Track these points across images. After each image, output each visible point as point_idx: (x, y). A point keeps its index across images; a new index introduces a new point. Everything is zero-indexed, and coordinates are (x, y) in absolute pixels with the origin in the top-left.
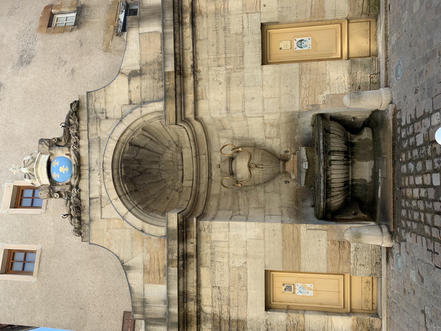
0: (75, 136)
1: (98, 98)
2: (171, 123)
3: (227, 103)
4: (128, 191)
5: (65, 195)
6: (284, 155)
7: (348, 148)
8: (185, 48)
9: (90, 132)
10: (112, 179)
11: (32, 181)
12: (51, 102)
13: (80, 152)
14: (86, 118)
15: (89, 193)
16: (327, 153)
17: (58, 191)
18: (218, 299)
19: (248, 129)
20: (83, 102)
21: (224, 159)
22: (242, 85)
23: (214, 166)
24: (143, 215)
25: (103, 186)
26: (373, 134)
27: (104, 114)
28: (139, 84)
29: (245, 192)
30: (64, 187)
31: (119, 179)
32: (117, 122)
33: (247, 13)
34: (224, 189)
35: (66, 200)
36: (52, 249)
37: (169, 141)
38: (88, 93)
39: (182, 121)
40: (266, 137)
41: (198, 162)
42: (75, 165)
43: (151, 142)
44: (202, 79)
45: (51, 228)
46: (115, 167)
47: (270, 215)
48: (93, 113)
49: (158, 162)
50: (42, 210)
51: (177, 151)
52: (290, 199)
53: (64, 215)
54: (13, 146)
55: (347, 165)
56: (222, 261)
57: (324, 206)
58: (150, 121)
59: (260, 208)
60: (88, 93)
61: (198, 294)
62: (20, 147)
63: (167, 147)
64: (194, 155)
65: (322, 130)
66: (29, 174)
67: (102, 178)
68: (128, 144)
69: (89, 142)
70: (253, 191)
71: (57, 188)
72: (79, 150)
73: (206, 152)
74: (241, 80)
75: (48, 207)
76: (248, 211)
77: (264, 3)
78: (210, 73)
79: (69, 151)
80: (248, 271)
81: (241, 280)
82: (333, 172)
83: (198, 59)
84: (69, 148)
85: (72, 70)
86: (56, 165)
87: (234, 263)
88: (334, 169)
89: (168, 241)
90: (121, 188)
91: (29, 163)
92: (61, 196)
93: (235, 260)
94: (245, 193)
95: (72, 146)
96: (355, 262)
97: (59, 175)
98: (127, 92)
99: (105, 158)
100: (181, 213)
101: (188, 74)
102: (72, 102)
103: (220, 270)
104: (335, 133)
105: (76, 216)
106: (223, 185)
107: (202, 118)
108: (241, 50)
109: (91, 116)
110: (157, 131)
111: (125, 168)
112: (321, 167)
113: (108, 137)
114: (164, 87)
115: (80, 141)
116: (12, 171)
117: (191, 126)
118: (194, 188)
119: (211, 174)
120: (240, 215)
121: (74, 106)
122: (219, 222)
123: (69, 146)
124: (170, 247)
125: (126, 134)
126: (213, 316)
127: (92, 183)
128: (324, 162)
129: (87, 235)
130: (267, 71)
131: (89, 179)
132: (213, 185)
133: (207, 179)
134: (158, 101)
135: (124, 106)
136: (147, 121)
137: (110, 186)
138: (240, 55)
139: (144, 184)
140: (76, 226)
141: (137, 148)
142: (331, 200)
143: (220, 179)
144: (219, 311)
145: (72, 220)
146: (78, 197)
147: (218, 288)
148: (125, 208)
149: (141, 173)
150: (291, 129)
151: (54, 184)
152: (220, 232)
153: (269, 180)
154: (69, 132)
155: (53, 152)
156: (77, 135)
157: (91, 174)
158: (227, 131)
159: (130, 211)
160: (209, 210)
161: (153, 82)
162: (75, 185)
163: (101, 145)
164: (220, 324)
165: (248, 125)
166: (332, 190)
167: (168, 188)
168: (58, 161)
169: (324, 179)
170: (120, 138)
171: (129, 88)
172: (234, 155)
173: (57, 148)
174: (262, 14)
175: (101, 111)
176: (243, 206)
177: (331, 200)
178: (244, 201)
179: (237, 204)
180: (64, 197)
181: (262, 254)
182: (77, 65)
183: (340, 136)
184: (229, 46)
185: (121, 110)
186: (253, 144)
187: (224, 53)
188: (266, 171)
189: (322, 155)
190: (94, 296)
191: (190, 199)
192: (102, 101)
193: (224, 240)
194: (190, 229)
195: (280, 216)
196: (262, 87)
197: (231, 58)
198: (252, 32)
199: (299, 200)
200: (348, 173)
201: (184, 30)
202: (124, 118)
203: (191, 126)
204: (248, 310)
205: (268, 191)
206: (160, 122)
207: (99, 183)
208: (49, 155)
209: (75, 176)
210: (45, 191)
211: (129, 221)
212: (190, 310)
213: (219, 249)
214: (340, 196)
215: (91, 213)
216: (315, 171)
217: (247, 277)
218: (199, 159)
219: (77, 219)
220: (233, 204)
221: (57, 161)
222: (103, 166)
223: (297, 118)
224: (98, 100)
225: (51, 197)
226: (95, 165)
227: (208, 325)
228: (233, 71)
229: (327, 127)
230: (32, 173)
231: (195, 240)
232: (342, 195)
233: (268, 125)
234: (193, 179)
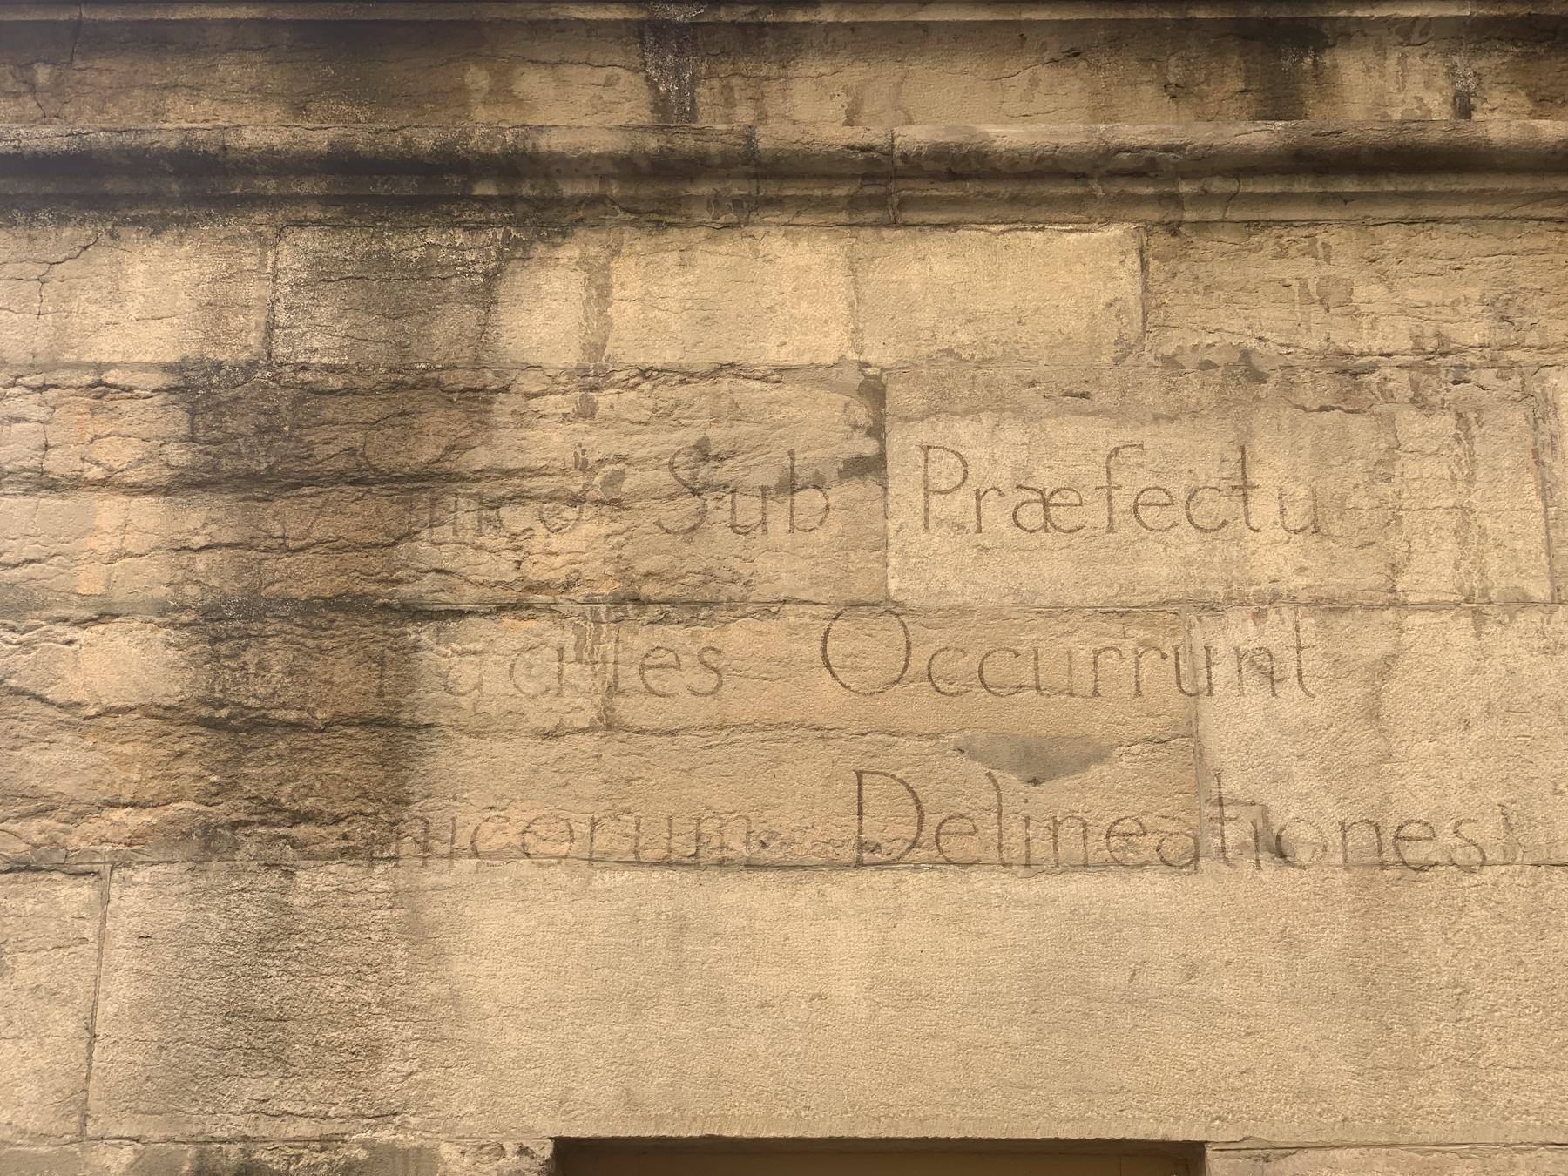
18: (702, 451)
56: (1263, 508)
61: (770, 189)
80: (1152, 888)
81: (1011, 781)
87: (1252, 681)
93: (1289, 691)
103: (1129, 486)
126: (463, 378)
144: (534, 459)
147: (869, 448)
164: (340, 478)
181: (1447, 1098)
204: (559, 875)
212: (531, 82)
213: (1430, 467)
217: (1060, 867)
227: (324, 314)
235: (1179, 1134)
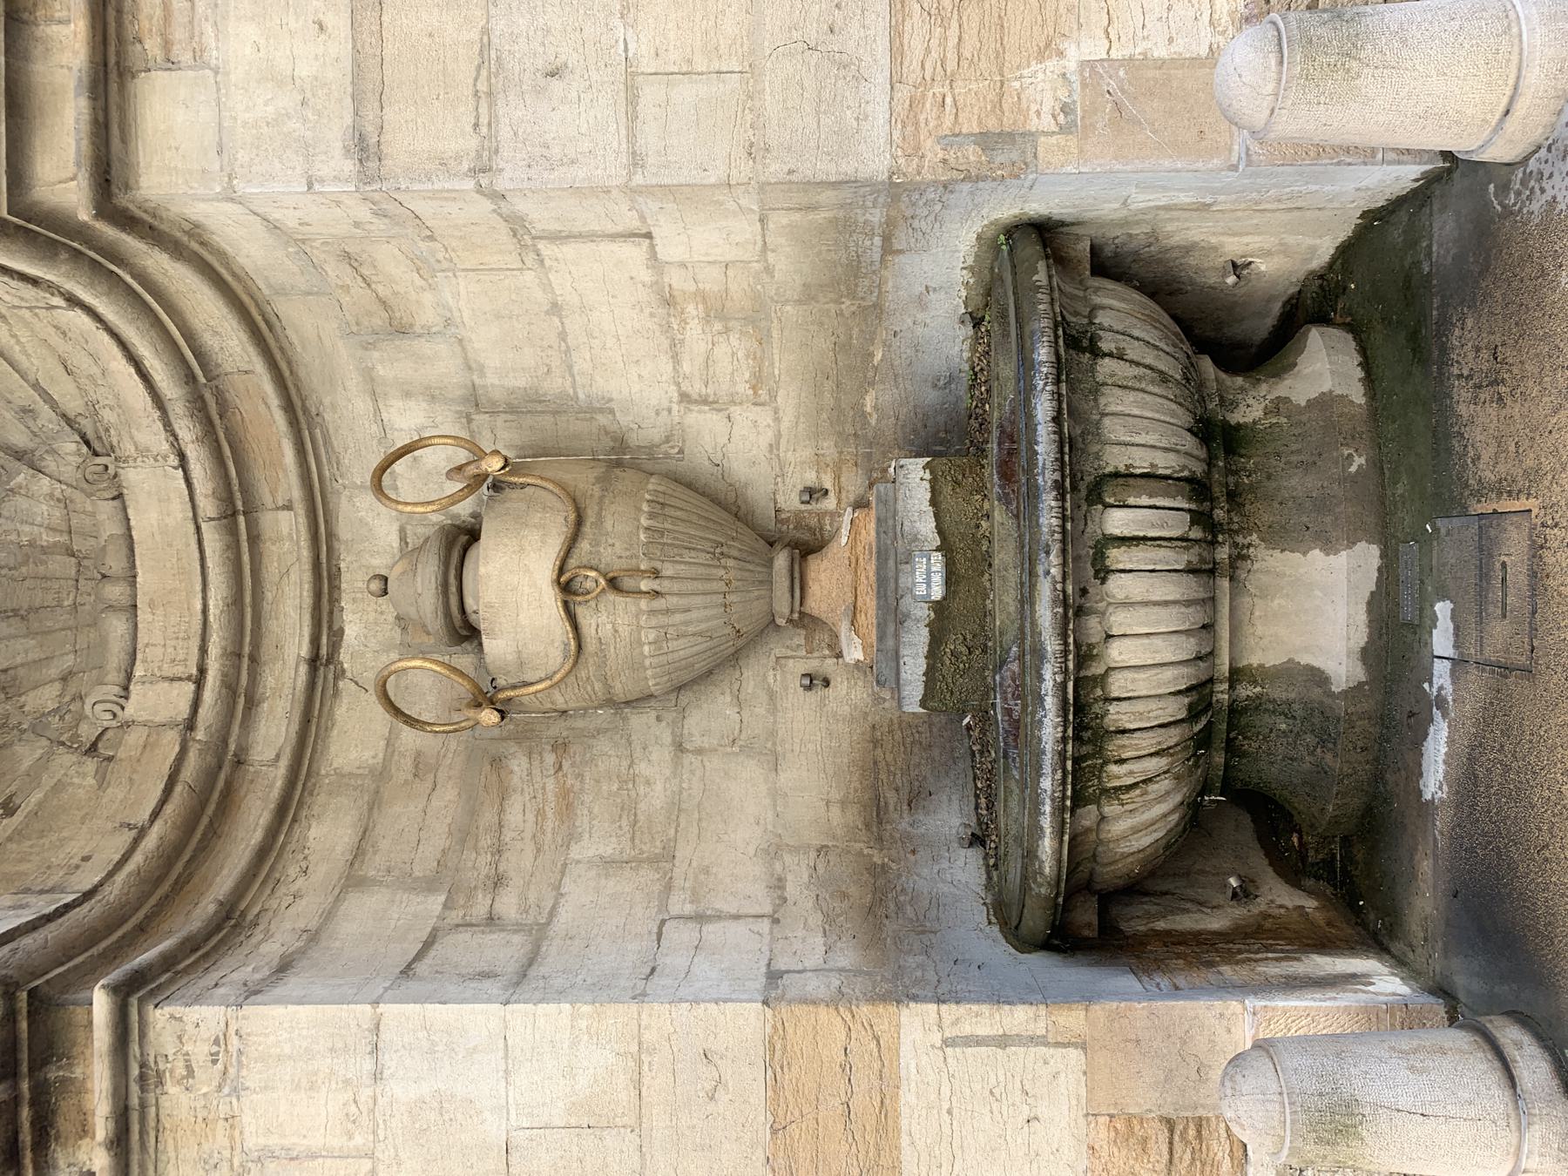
6: (798, 513)
7: (1210, 462)
16: (1083, 487)
19: (563, 336)
21: (416, 534)
23: (353, 581)
26: (1366, 365)
29: (554, 748)
34: (408, 735)
37: (27, 412)
40: (684, 397)
41: (246, 558)
47: (700, 918)
52: (836, 795)
55: (1205, 571)
57: (1059, 861)
59: (635, 862)
63: (19, 455)
64: (208, 507)
65: (1045, 323)
70: (603, 745)
73: (297, 494)
82: (1119, 621)
88: (1127, 604)
94: (550, 758)
104: (1131, 355)
107: (196, 230)
112: (1045, 591)
118: (200, 735)
119: (337, 635)
120: (492, 921)
122: (305, 1011)
128: (1064, 551)
132: (341, 711)
133: (303, 669)
142: (1103, 818)
150: (841, 347)
152: (312, 1087)
153: (710, 672)
158: (424, 347)
160: (282, 890)
165: (555, 308)
166: (1114, 747)
167: (29, 735)
169: (1065, 671)
176: (530, 849)
177: (1103, 818)
178: (540, 813)
179: (486, 841)
183: (1164, 378)
188: (678, 618)
189: (1049, 500)
191: (155, 815)
193: (336, 1142)
194: (78, 1072)
195: (765, 926)
199: (891, 797)
200: (1208, 627)
205: (698, 741)
214: (1165, 784)
216: (986, 614)
218: (254, 539)
220: (464, 835)
223: (877, 257)
229: (1076, 314)
232: (1177, 778)
234: (202, 671)
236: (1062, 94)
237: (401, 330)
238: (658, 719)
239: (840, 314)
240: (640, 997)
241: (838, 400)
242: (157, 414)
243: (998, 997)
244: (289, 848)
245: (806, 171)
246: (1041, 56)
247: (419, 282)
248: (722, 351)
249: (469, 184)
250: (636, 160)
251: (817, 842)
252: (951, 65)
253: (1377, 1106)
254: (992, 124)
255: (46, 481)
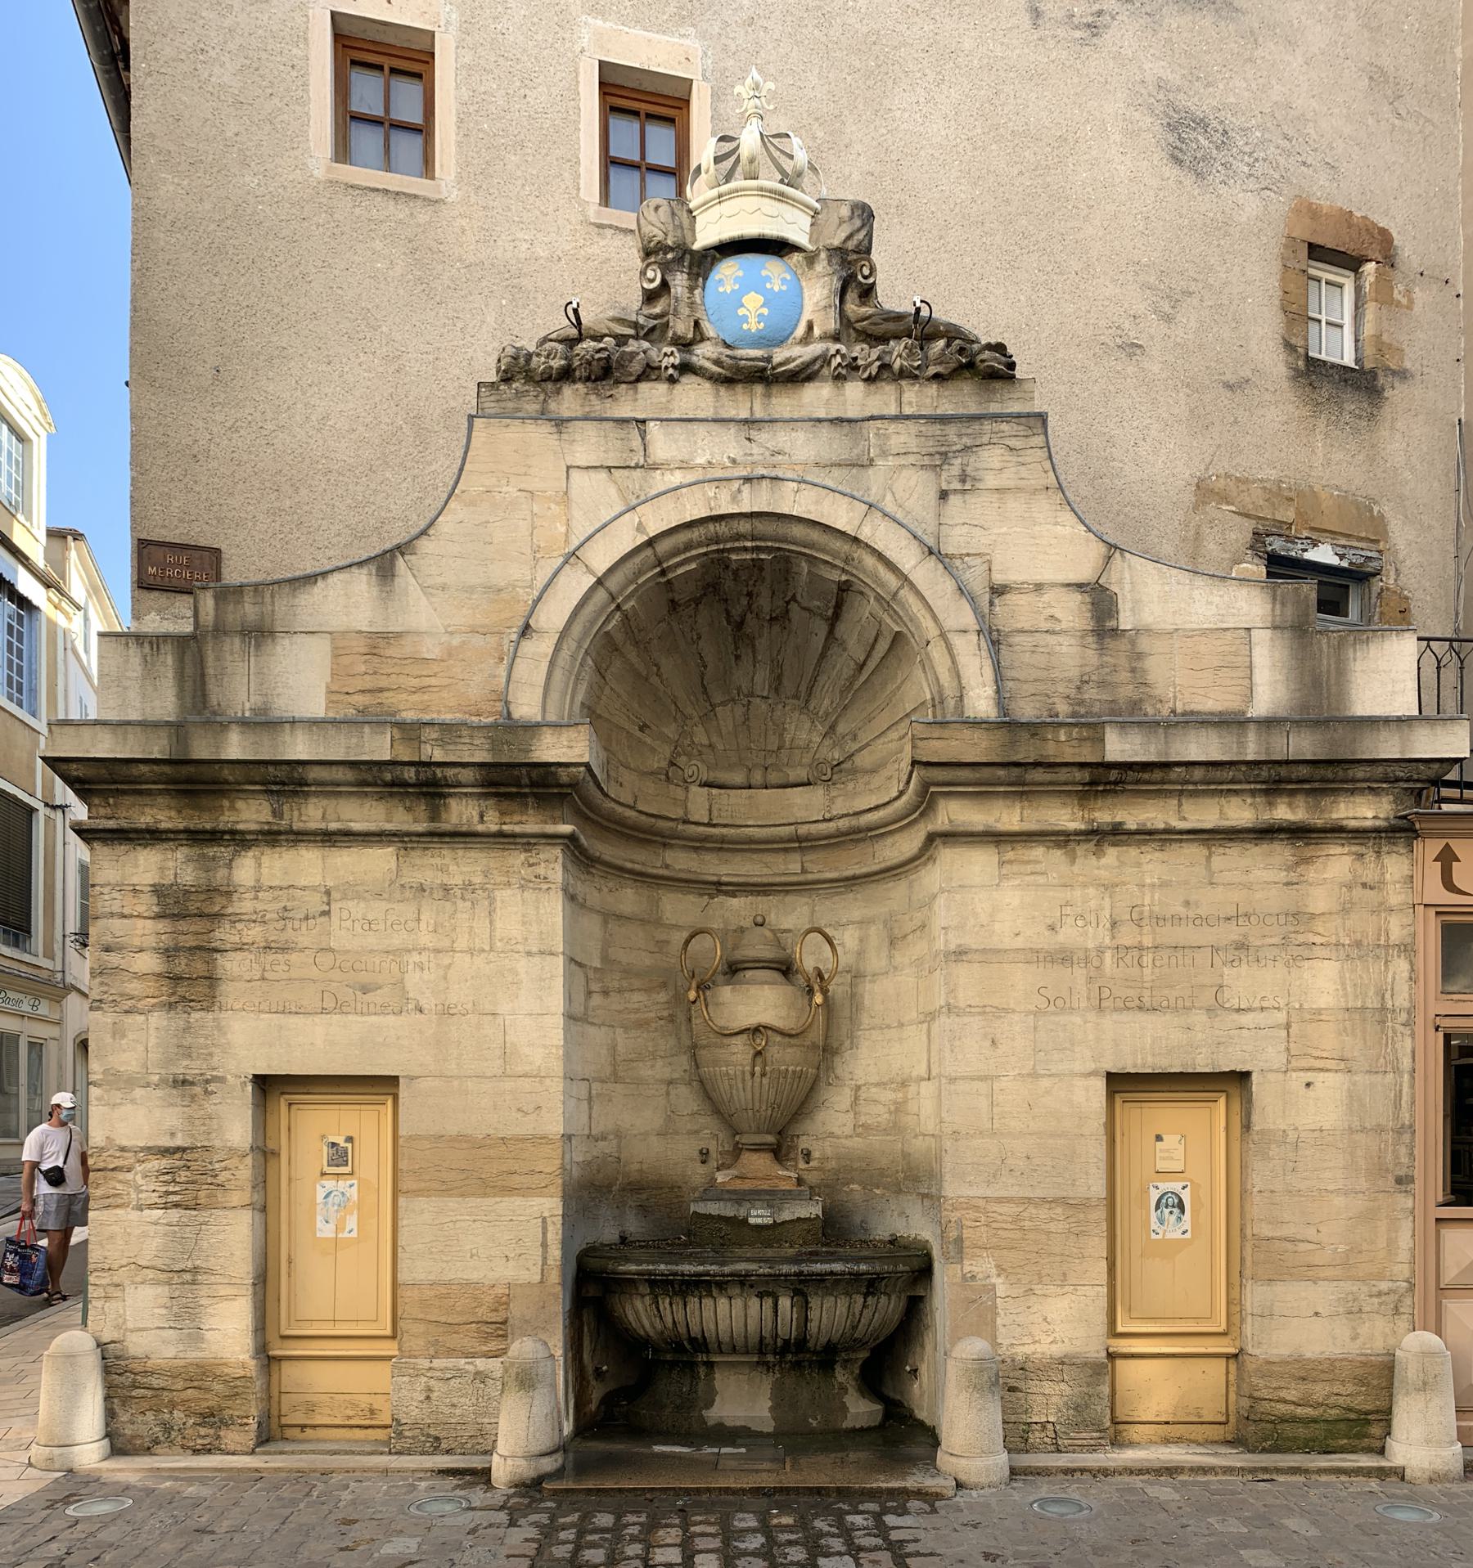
0: (878, 363)
1: (1020, 459)
2: (919, 743)
3: (984, 951)
4: (671, 576)
5: (656, 317)
6: (796, 1147)
7: (815, 1352)
8: (1184, 801)
9: (892, 427)
10: (714, 513)
11: (707, 173)
12: (1018, 252)
13: (817, 384)
14: (947, 408)
15: (662, 420)
16: (801, 1286)
17: (671, 283)
18: (285, 909)
19: (889, 1027)
20: (1007, 396)
22: (1042, 1006)
24: (585, 634)
25: (690, 478)
26: (862, 1429)
27: (959, 486)
28: (1064, 626)
30: (687, 311)
31: (717, 540)
32: (925, 538)
33: (1288, 1026)
34: (679, 937)
35: (634, 318)
36: (441, 248)
38: (1042, 418)
39: (925, 786)
40: (858, 1088)
42: (769, 359)
43: (852, 663)
44: (1073, 861)
45: (525, 246)
46: (762, 527)
48: (966, 441)
49: (777, 690)
50: (596, 207)
51: (816, 764)
52: (645, 1167)
53: (576, 311)
54: (849, 78)
55: (761, 1347)
56: (423, 925)
57: (625, 1273)
58: (927, 665)
59: (614, 1065)
60: (1042, 418)
61: (300, 837)
62: (846, 112)
65: (878, 1269)
66: (735, 156)
67: (719, 474)
68: (844, 578)
69: (856, 421)
70: (672, 1041)
71: (679, 282)
72: (824, 379)
74: (1059, 1002)
75: (608, 232)
76: (603, 1024)
77: (1318, 1085)
78: (1091, 891)
79: (824, 337)
80: (391, 1019)
81: (358, 993)
82: (738, 1303)
83: (1143, 848)
84: (836, 338)
85: (1138, 346)
86: (768, 279)
87: (417, 970)
88: (746, 1307)
89: (494, 726)
90: (682, 546)
91: (776, 154)
92: (650, 297)
93: (426, 971)
95: (844, 350)
96: (439, 1374)
97: (733, 291)
98: (1038, 578)
99: (795, 485)
100: (589, 778)
101: (1093, 810)
102: (1010, 350)
103: (391, 918)
104: (865, 1311)
105: (576, 363)
106: (692, 936)
108: (1165, 1004)
109: (951, 430)
110: (891, 687)
111: (757, 564)
112: (752, 1267)
113: (870, 500)
114: (1049, 720)
115: (861, 383)
116: (749, 81)
117: (906, 821)
120: (589, 993)
121: (995, 359)
123: (844, 337)
124: (464, 733)
125: (883, 571)
126: (225, 889)
127: (701, 429)
128: (770, 1275)
129: (503, 404)
130: (1087, 1090)
131: (715, 421)
134: (1001, 699)
135: (986, 566)
136: (927, 654)
137: (688, 507)
138: (1146, 1000)
139: (699, 638)
140: (535, 359)
141: (830, 613)
142: (643, 1296)
143: (716, 926)
144: (243, 911)
145: (560, 341)
146: (650, 372)
147: (327, 908)
148: (608, 565)
149: (740, 625)
150: (882, 1172)
151: (695, 270)
153: (710, 1098)
154: (898, 337)
155: (821, 266)
156: (884, 373)
157: (733, 428)
158: (884, 954)
159: (600, 582)
161: (1070, 681)
162: (694, 359)
163: (845, 471)
164: (195, 915)
165: (901, 1025)
166: (678, 1300)
167: (681, 730)
168: (784, 288)
169: (714, 1276)
170: (867, 545)
171: (1053, 585)
172: (799, 976)
173: (837, 284)
174: (1281, 1076)
175: (969, 470)
176: (620, 1008)
177: (643, 1296)
178: (637, 1011)
179: (625, 984)
180: (647, 311)
181: (454, 1066)
182: (1156, 368)
183: (854, 1328)
184: (1180, 962)
185: (971, 552)
186: (835, 1045)
187: (1159, 941)
188: (740, 1085)
189: (794, 1269)
190: (270, 426)
191: (640, 812)
192: (1006, 479)
196: (1029, 1075)
197: (1137, 969)
198: (1223, 1040)
199: (644, 1196)
200: (734, 1350)
201: (1249, 801)
202: (940, 566)
203: (906, 821)
204: (252, 1015)
205: (673, 1092)
206: (923, 703)
207: (701, 460)
208: (810, 247)
209: (729, 361)
210: (671, 228)
211: (562, 579)
212: (240, 804)
213: (465, 916)
214: (659, 1326)
215: (588, 425)
216: (741, 1246)
217: (369, 1014)
219: (563, 366)
220: (627, 972)
221: (784, 280)
222: (763, 477)
223: (921, 1191)
224: (1015, 459)
225: (648, 253)
226: (768, 445)
227: (189, 870)
228: (1092, 974)
229: (886, 1286)
230: (739, 169)
231: (494, 828)
232: (662, 1332)
233: (900, 1095)
235: (393, 1074)
236: (980, 1276)
237: (893, 942)
238: (685, 1071)
239: (897, 1172)
240: (565, 1078)
241: (856, 1170)
242: (851, 812)
243: (565, 1244)
244: (623, 881)
245: (947, 1158)
246: (998, 1266)
247: (914, 958)
248: (880, 1109)
249: (943, 1004)
250: (952, 1080)
251: (622, 1156)
252: (994, 1225)
253: (532, 1398)
254: (967, 1243)
255: (819, 740)
